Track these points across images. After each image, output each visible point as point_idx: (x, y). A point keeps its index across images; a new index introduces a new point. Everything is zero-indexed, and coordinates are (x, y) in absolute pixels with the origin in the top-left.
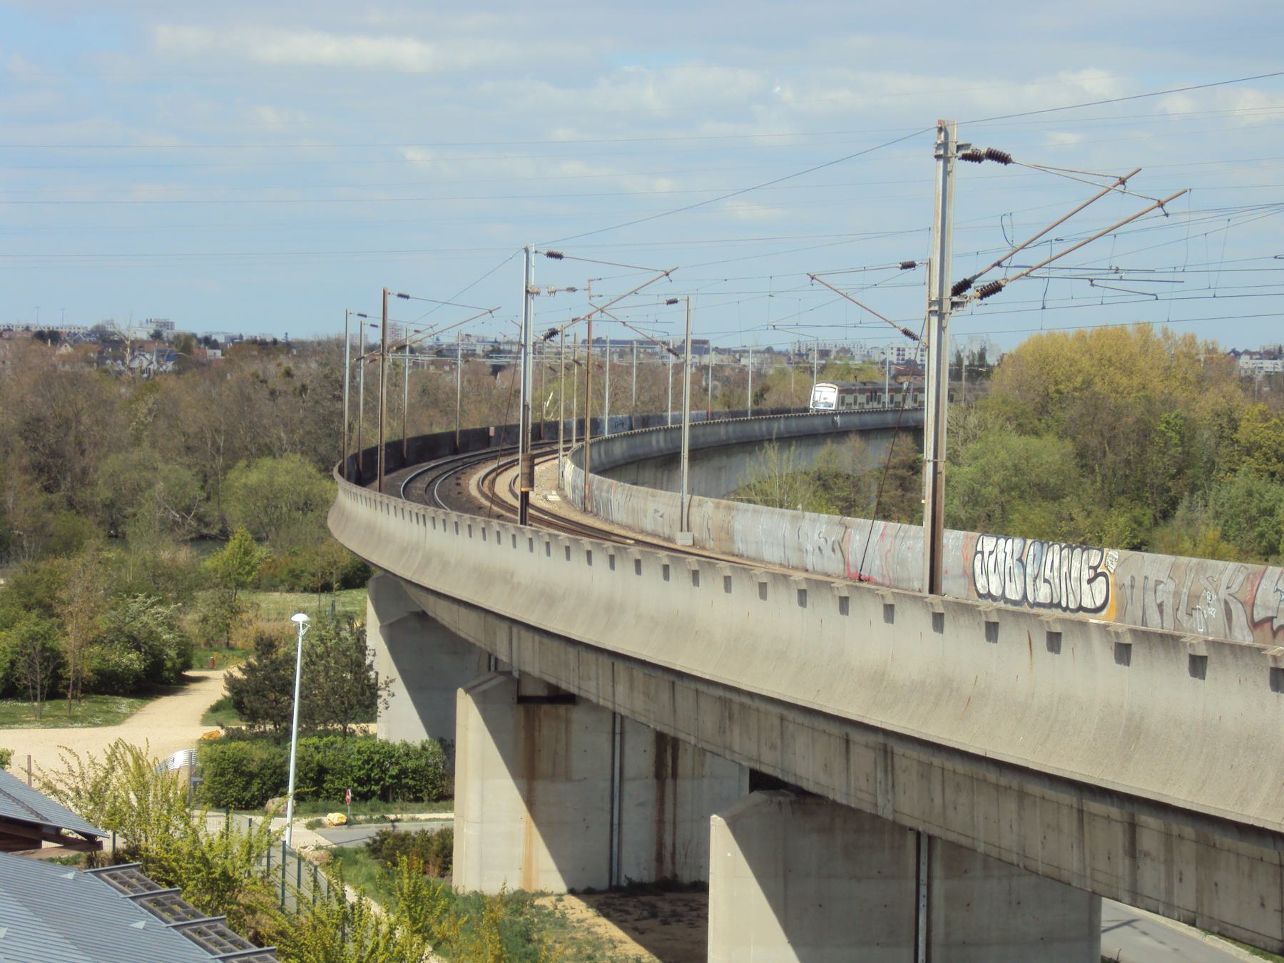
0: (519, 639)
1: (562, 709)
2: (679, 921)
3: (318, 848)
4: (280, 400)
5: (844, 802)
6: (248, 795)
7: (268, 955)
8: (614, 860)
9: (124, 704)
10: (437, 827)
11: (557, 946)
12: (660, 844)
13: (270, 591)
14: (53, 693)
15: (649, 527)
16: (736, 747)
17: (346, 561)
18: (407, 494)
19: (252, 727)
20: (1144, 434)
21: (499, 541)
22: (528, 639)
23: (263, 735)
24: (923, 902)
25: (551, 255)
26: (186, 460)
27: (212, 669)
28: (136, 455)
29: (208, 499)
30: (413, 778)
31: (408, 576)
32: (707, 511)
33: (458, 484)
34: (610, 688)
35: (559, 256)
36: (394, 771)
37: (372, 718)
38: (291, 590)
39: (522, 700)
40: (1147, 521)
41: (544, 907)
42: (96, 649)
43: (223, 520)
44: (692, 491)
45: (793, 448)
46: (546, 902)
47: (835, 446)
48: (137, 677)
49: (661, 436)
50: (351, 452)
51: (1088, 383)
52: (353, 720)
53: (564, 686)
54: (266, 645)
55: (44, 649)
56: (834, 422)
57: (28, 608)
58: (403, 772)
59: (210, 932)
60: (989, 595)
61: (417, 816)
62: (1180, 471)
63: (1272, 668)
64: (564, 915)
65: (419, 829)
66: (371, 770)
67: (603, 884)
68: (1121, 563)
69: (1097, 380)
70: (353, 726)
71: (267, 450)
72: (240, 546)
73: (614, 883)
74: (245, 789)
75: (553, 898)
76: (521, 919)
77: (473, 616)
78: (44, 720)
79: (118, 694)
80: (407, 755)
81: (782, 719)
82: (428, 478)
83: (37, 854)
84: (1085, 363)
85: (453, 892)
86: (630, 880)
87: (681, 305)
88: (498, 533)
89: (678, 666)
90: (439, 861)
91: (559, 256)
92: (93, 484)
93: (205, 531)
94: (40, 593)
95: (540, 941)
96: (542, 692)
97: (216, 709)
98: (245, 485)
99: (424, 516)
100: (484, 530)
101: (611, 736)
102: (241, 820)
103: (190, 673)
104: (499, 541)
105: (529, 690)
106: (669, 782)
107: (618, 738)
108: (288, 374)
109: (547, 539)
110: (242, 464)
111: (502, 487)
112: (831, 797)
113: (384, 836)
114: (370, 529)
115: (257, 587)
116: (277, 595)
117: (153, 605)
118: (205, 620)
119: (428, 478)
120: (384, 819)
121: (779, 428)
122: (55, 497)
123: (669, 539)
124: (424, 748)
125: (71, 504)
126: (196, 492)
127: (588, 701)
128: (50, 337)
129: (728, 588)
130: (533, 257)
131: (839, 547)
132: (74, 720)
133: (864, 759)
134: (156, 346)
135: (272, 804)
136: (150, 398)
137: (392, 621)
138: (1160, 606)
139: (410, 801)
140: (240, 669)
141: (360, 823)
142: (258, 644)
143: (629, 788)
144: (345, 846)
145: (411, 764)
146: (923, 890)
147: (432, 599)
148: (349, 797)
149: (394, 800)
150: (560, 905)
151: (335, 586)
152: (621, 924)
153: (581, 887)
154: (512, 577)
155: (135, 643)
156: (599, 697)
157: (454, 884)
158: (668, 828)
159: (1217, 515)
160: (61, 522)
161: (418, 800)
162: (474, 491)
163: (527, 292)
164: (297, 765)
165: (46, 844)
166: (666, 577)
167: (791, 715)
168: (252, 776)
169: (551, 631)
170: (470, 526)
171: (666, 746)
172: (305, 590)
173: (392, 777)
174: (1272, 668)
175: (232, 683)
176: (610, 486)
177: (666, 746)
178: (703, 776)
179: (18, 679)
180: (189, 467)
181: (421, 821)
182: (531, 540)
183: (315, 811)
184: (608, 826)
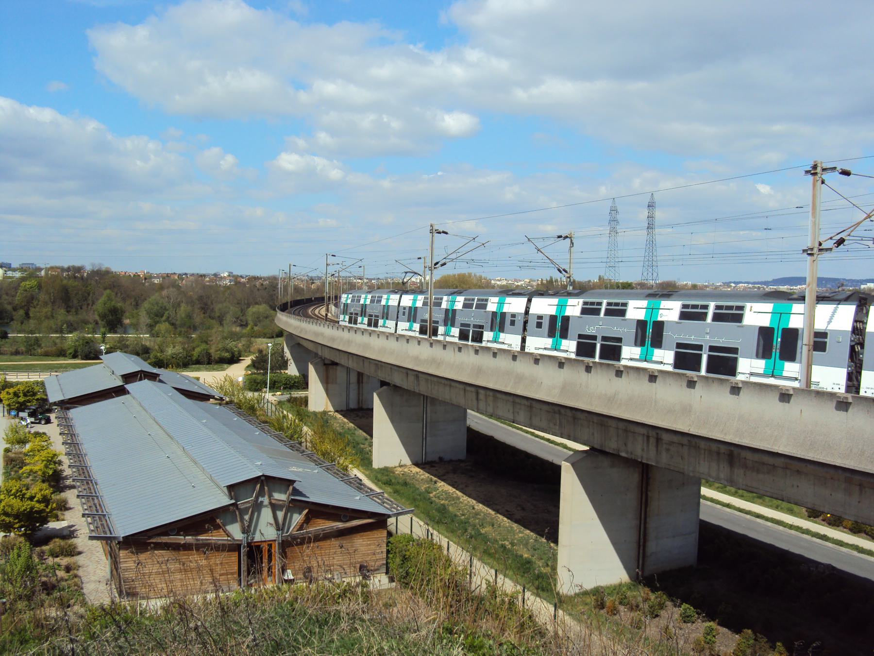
1: (335, 367)
8: (348, 404)
9: (225, 366)
10: (304, 395)
12: (359, 399)
14: (209, 363)
17: (277, 330)
18: (294, 314)
22: (326, 349)
23: (260, 373)
28: (225, 304)
31: (297, 334)
35: (334, 256)
36: (293, 382)
38: (264, 338)
39: (325, 364)
42: (219, 352)
48: (228, 359)
53: (335, 361)
54: (260, 351)
55: (207, 352)
58: (295, 382)
67: (345, 409)
71: (256, 303)
78: (207, 370)
81: (391, 369)
82: (298, 310)
83: (209, 402)
84: (455, 282)
87: (363, 268)
89: (367, 355)
91: (334, 256)
92: (215, 312)
96: (329, 362)
97: (248, 367)
102: (256, 394)
103: (241, 358)
105: (326, 362)
106: (361, 385)
108: (262, 285)
110: (251, 306)
111: (317, 312)
113: (291, 397)
114: (286, 323)
115: (256, 337)
118: (244, 345)
119: (298, 310)
122: (205, 315)
125: (210, 317)
126: (239, 313)
128: (203, 276)
129: (378, 337)
132: (214, 370)
133: (411, 378)
134: (229, 278)
136: (228, 292)
143: (351, 386)
144: (282, 400)
145: (296, 380)
146: (425, 409)
147: (301, 339)
155: (227, 351)
158: (361, 395)
161: (299, 389)
162: (310, 314)
165: (211, 400)
166: (363, 335)
167: (393, 367)
168: (258, 383)
171: (360, 375)
175: (252, 360)
177: (360, 375)
180: (238, 308)
183: (273, 392)
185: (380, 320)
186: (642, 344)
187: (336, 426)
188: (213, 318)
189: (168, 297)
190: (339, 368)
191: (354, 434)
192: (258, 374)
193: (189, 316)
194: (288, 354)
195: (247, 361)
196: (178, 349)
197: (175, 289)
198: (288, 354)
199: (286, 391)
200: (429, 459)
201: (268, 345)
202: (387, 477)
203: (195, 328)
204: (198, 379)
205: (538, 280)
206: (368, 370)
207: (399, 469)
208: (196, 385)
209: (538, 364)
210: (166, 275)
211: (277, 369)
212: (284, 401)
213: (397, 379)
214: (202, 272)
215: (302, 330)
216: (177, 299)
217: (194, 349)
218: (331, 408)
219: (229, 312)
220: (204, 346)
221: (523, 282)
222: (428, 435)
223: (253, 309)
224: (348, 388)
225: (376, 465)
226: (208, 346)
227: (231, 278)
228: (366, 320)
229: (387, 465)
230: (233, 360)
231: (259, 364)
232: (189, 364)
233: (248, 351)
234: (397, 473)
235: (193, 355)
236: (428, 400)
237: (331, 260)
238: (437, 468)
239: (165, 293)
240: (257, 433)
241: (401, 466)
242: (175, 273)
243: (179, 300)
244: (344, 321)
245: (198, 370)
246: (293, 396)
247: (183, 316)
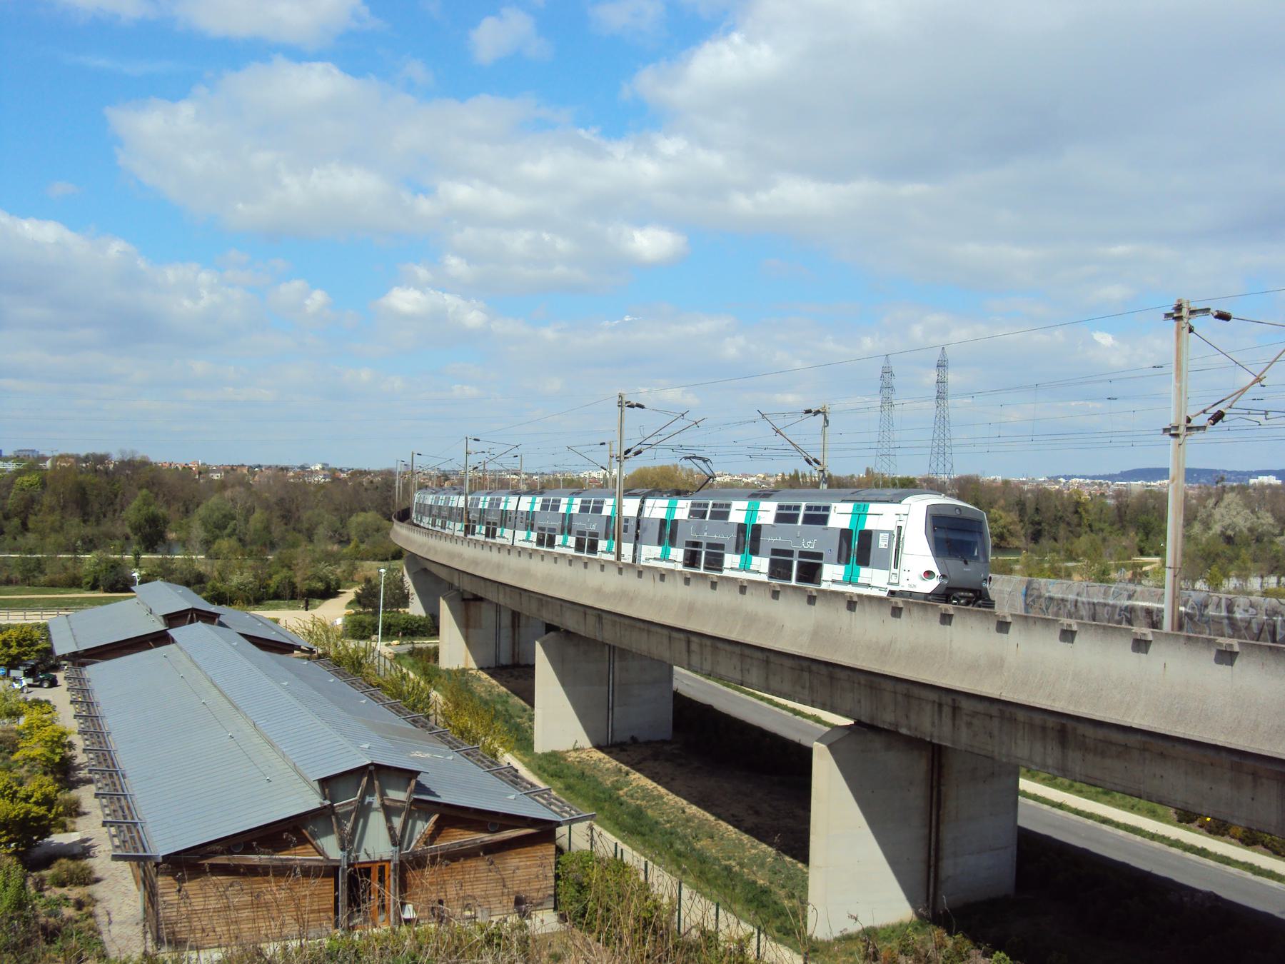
1: (478, 603)
8: (497, 657)
9: (317, 602)
10: (432, 645)
14: (293, 597)
17: (393, 549)
22: (466, 578)
25: (475, 440)
26: (335, 513)
28: (317, 511)
31: (422, 555)
35: (478, 440)
36: (416, 625)
38: (374, 560)
39: (464, 600)
42: (307, 581)
43: (348, 535)
46: (473, 672)
48: (321, 591)
53: (479, 594)
54: (368, 581)
55: (289, 582)
57: (283, 567)
64: (479, 677)
67: (494, 666)
70: (401, 610)
71: (364, 510)
78: (290, 607)
81: (561, 606)
87: (519, 457)
89: (525, 586)
91: (478, 440)
94: (287, 562)
96: (471, 597)
97: (351, 603)
102: (362, 644)
108: (372, 482)
110: (355, 514)
113: (414, 648)
114: (408, 539)
115: (362, 559)
116: (368, 562)
118: (344, 571)
122: (289, 527)
125: (294, 529)
126: (338, 525)
127: (488, 600)
128: (286, 469)
129: (543, 560)
133: (591, 620)
134: (323, 472)
135: (374, 637)
144: (401, 652)
145: (422, 623)
147: (429, 562)
153: (486, 666)
155: (321, 580)
160: (290, 537)
161: (425, 636)
164: (382, 625)
165: (295, 652)
166: (520, 556)
167: (564, 604)
171: (516, 616)
175: (357, 594)
177: (516, 616)
180: (336, 516)
183: (388, 640)
185: (600, 541)
186: (847, 562)
187: (480, 690)
188: (300, 531)
189: (232, 500)
190: (484, 605)
191: (507, 702)
192: (365, 614)
193: (267, 528)
195: (350, 594)
196: (247, 577)
197: (242, 489)
199: (406, 638)
200: (618, 739)
201: (379, 571)
202: (555, 766)
203: (272, 546)
204: (276, 621)
205: (777, 475)
206: (527, 608)
207: (574, 754)
208: (272, 628)
209: (777, 599)
210: (229, 468)
211: (393, 606)
212: (404, 654)
213: (570, 622)
215: (429, 549)
216: (246, 503)
217: (270, 577)
218: (472, 665)
219: (322, 523)
220: (285, 572)
221: (754, 479)
222: (615, 704)
223: (358, 519)
224: (498, 634)
225: (540, 747)
226: (291, 573)
227: (326, 472)
228: (572, 541)
229: (556, 749)
230: (329, 592)
231: (366, 599)
232: (263, 599)
233: (350, 580)
234: (569, 759)
235: (269, 585)
236: (617, 651)
237: (473, 446)
238: (629, 753)
239: (228, 494)
240: (364, 701)
241: (576, 750)
242: (243, 465)
243: (249, 504)
244: (564, 545)
245: (277, 608)
246: (417, 646)
247: (259, 526)
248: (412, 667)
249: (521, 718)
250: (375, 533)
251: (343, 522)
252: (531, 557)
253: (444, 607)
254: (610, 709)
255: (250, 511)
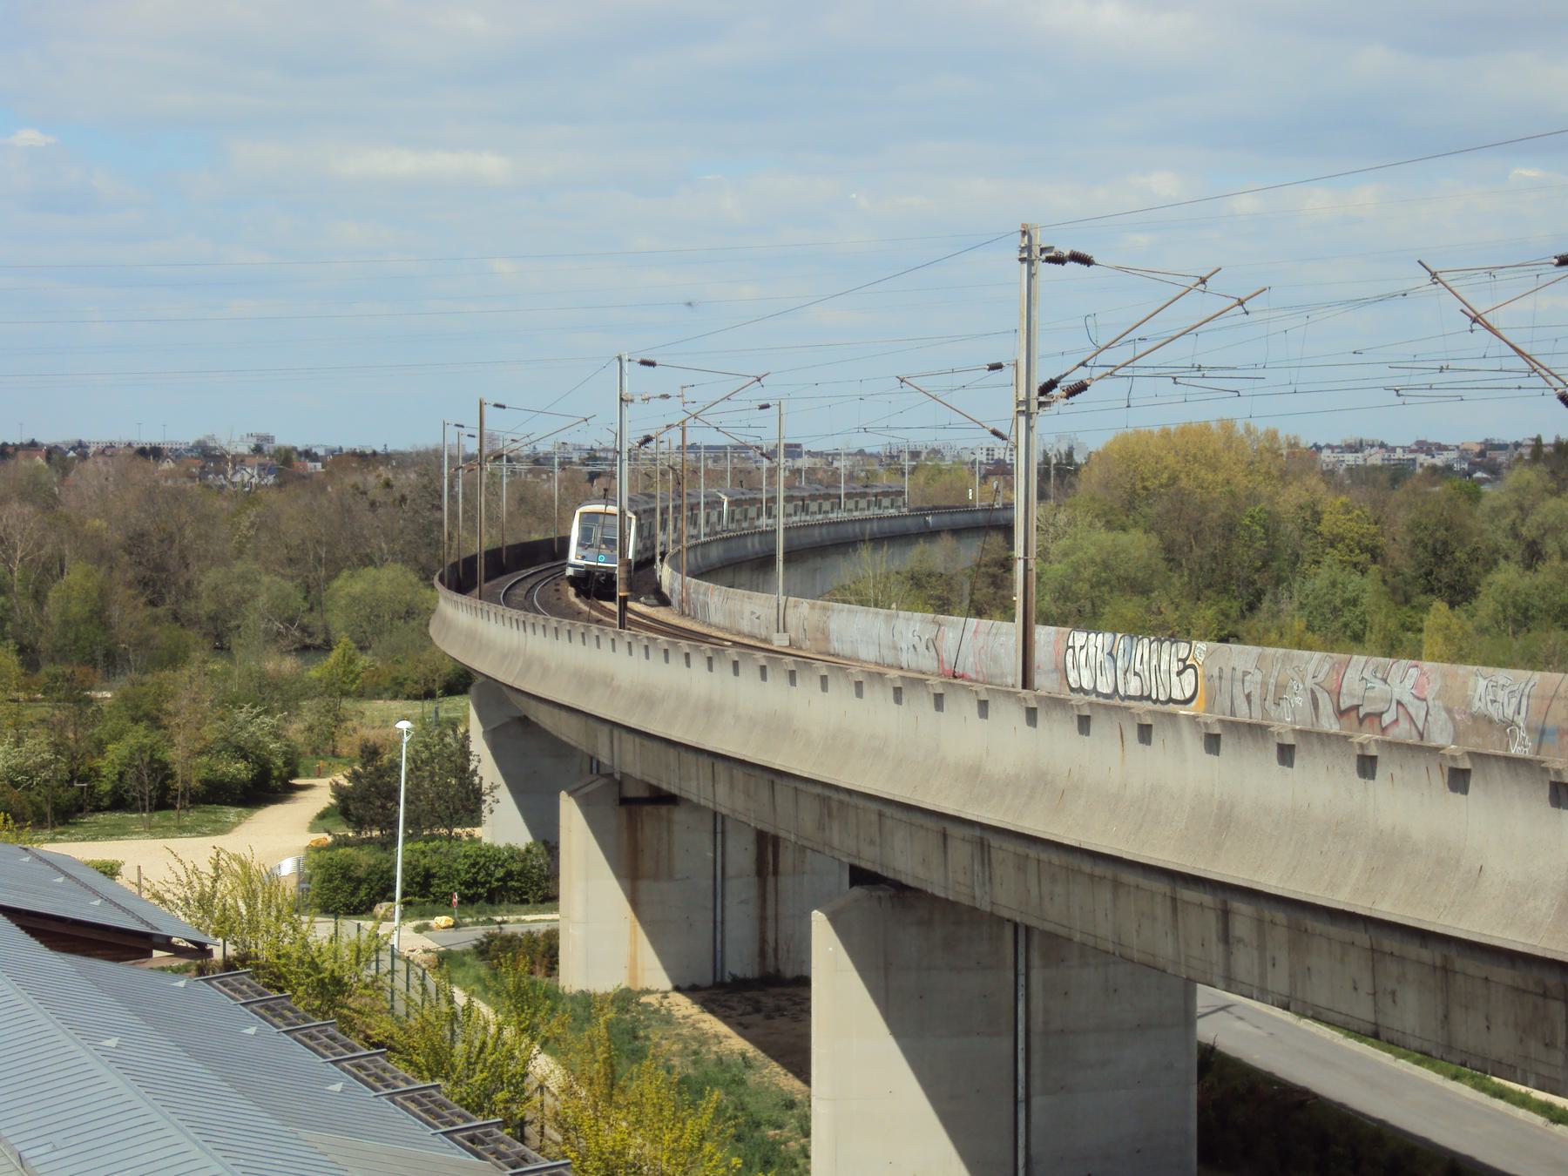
0: (620, 738)
1: (664, 810)
2: (783, 1015)
3: (426, 951)
4: (381, 511)
5: (942, 895)
6: (356, 901)
7: (378, 1058)
9: (232, 813)
10: (543, 928)
11: (664, 1042)
12: (763, 940)
13: (374, 699)
15: (746, 628)
16: (836, 843)
17: (448, 668)
18: (507, 601)
19: (359, 833)
20: (1229, 528)
21: (598, 646)
22: (629, 744)
24: (1021, 992)
25: (644, 363)
26: (288, 571)
27: (319, 777)
28: (239, 567)
29: (311, 609)
30: (518, 881)
31: (509, 681)
32: (803, 612)
33: (557, 590)
34: (711, 788)
35: (652, 364)
36: (500, 873)
37: (477, 823)
38: (395, 697)
39: (624, 801)
40: (1234, 613)
41: (650, 1004)
42: (205, 759)
43: (326, 630)
44: (787, 593)
45: (885, 548)
47: (927, 546)
48: (245, 787)
49: (756, 539)
50: (453, 559)
51: (1174, 479)
52: (458, 825)
53: (665, 786)
54: (370, 753)
56: (926, 522)
58: (509, 875)
59: (321, 1036)
60: (1081, 689)
61: (523, 917)
62: (1265, 564)
63: (1358, 756)
64: (669, 1011)
65: (525, 930)
66: (477, 873)
67: (707, 979)
68: (1210, 654)
69: (1182, 476)
70: (457, 830)
71: (367, 561)
72: (344, 656)
73: (718, 979)
74: (353, 894)
75: (659, 996)
76: (628, 1016)
77: (574, 720)
78: (153, 831)
79: (226, 804)
80: (512, 857)
81: (881, 815)
83: (149, 963)
84: (1170, 460)
85: (560, 991)
86: (734, 978)
87: (774, 410)
88: (597, 637)
89: (778, 763)
90: (546, 961)
91: (652, 364)
92: (197, 597)
93: (308, 641)
94: (147, 706)
95: (647, 1038)
96: (644, 793)
97: (322, 816)
98: (348, 594)
99: (524, 622)
100: (583, 634)
101: (712, 837)
102: (349, 926)
104: (598, 646)
105: (631, 791)
106: (771, 879)
107: (719, 837)
108: (388, 485)
109: (646, 642)
110: (345, 573)
112: (929, 891)
113: (491, 938)
114: (471, 636)
115: (361, 695)
116: (382, 702)
117: (257, 716)
118: (310, 729)
120: (490, 921)
121: (871, 529)
122: (160, 611)
123: (765, 640)
124: (528, 851)
125: (176, 618)
126: (298, 601)
127: (688, 801)
128: (153, 453)
129: (824, 688)
130: (626, 365)
131: (933, 644)
132: (182, 830)
133: (961, 853)
134: (258, 459)
135: (381, 909)
136: (252, 513)
137: (495, 726)
138: (1248, 697)
139: (516, 903)
140: (345, 776)
141: (466, 925)
142: (363, 751)
144: (453, 948)
145: (516, 867)
146: (1022, 980)
147: (533, 703)
148: (455, 900)
149: (500, 902)
150: (665, 1002)
151: (439, 693)
152: (725, 1019)
153: (686, 985)
154: (612, 679)
155: (242, 753)
156: (699, 796)
157: (561, 983)
158: (770, 924)
159: (1302, 606)
160: (164, 635)
161: (526, 902)
163: (622, 399)
164: (404, 870)
165: (156, 953)
166: (764, 677)
167: (888, 811)
168: (360, 881)
169: (652, 732)
170: (569, 632)
171: (767, 845)
172: (408, 698)
173: (498, 880)
174: (1358, 756)
175: (337, 789)
176: (708, 588)
177: (767, 845)
178: (803, 873)
179: (127, 791)
180: (292, 578)
181: (527, 922)
182: (629, 643)
183: (422, 915)
184: (712, 925)
190: (679, 815)
191: (741, 1082)
192: (364, 842)
193: (99, 616)
194: (486, 768)
195: (319, 795)
197: (28, 509)
198: (486, 768)
199: (471, 910)
203: (112, 662)
204: (110, 870)
208: (96, 894)
211: (441, 821)
214: (149, 436)
215: (528, 665)
216: (40, 546)
217: (100, 747)
220: (138, 735)
222: (1036, 1084)
223: (351, 586)
226: (156, 736)
232: (81, 809)
233: (325, 750)
235: (96, 772)
236: (1036, 940)
240: (338, 1087)
242: (33, 445)
243: (48, 549)
247: (77, 609)
248: (486, 989)
249: (780, 1127)
250: (400, 623)
251: (313, 594)
252: (793, 681)
253: (572, 819)
254: (1021, 1101)
255: (52, 569)
